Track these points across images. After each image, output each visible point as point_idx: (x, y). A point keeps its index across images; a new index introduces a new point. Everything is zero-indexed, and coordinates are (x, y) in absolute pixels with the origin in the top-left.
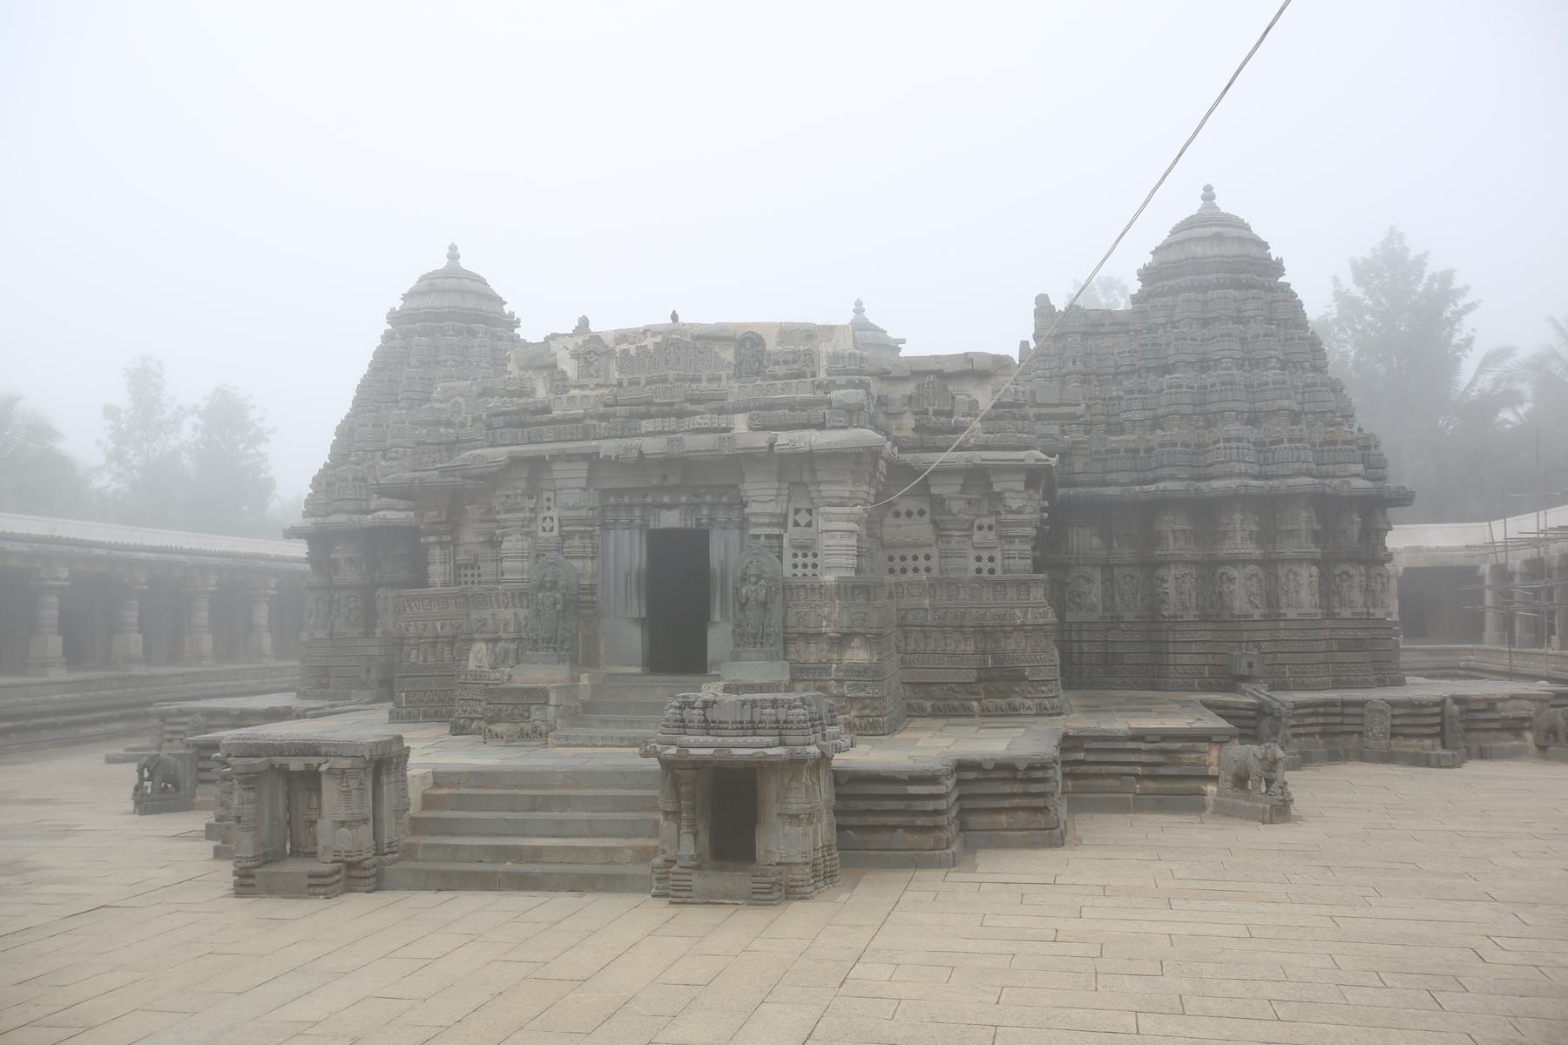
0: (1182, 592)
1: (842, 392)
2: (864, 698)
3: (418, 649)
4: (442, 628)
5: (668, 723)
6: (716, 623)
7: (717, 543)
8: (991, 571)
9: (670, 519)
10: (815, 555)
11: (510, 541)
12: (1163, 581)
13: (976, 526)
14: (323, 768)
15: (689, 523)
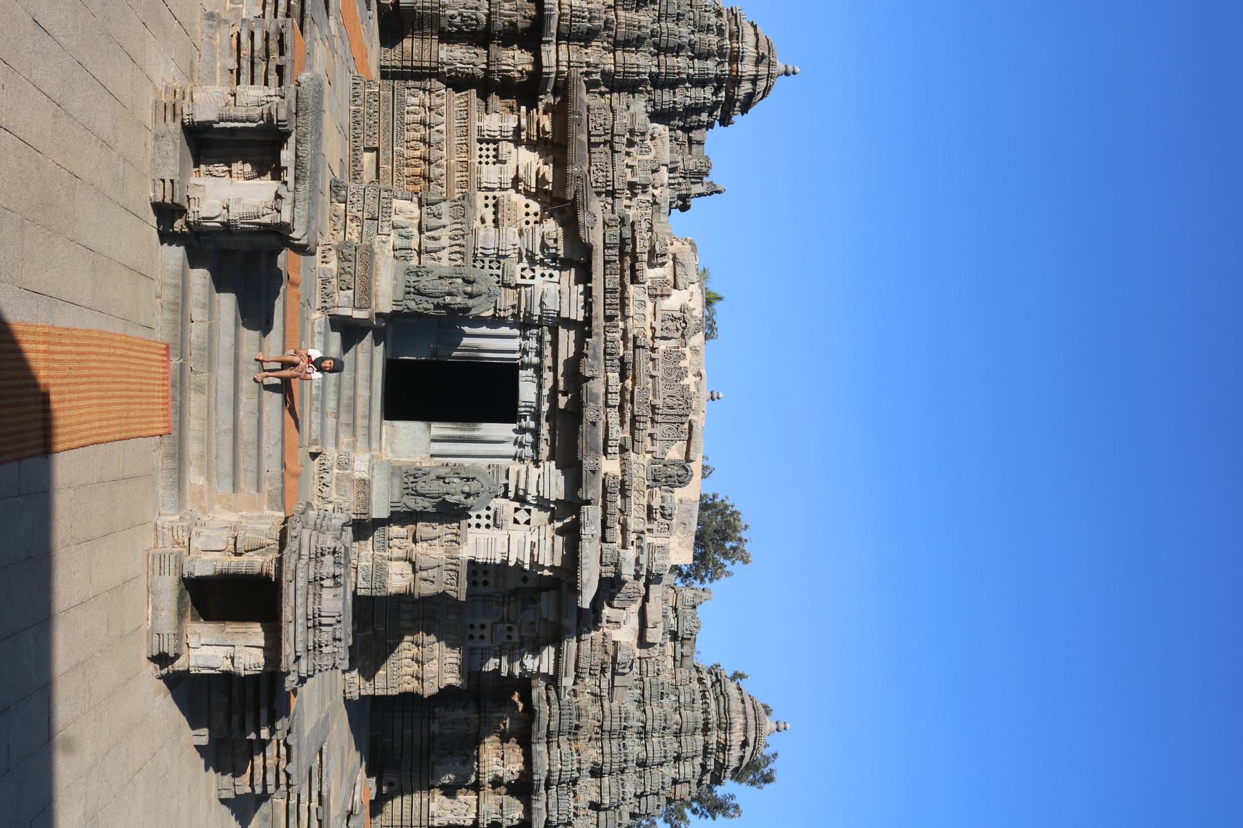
0: (454, 723)
1: (633, 562)
2: (357, 578)
3: (419, 106)
4: (438, 131)
5: (321, 540)
6: (430, 430)
7: (504, 430)
8: (472, 637)
9: (527, 391)
10: (488, 526)
11: (514, 238)
12: (464, 707)
13: (511, 625)
14: (283, 192)
15: (523, 409)
